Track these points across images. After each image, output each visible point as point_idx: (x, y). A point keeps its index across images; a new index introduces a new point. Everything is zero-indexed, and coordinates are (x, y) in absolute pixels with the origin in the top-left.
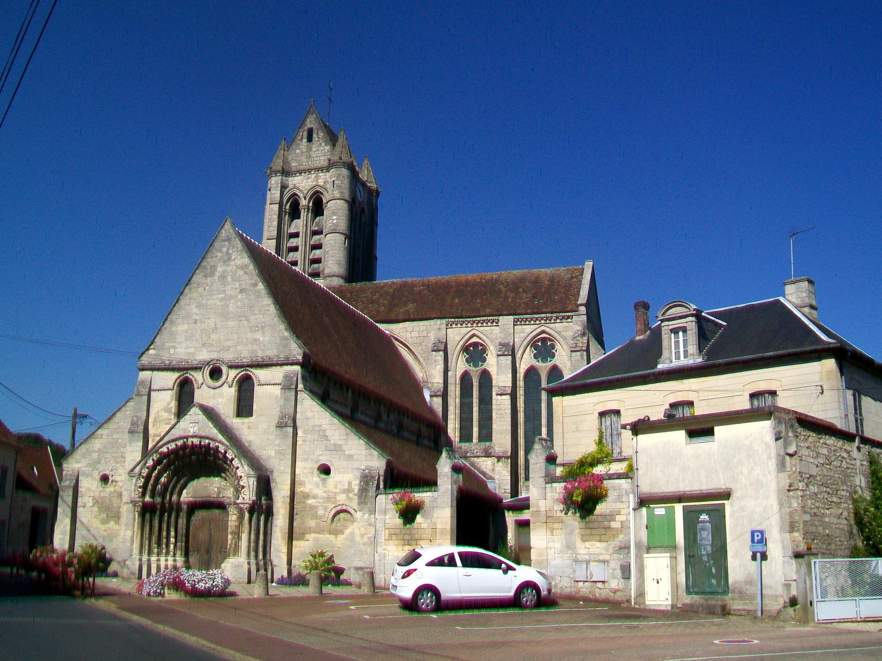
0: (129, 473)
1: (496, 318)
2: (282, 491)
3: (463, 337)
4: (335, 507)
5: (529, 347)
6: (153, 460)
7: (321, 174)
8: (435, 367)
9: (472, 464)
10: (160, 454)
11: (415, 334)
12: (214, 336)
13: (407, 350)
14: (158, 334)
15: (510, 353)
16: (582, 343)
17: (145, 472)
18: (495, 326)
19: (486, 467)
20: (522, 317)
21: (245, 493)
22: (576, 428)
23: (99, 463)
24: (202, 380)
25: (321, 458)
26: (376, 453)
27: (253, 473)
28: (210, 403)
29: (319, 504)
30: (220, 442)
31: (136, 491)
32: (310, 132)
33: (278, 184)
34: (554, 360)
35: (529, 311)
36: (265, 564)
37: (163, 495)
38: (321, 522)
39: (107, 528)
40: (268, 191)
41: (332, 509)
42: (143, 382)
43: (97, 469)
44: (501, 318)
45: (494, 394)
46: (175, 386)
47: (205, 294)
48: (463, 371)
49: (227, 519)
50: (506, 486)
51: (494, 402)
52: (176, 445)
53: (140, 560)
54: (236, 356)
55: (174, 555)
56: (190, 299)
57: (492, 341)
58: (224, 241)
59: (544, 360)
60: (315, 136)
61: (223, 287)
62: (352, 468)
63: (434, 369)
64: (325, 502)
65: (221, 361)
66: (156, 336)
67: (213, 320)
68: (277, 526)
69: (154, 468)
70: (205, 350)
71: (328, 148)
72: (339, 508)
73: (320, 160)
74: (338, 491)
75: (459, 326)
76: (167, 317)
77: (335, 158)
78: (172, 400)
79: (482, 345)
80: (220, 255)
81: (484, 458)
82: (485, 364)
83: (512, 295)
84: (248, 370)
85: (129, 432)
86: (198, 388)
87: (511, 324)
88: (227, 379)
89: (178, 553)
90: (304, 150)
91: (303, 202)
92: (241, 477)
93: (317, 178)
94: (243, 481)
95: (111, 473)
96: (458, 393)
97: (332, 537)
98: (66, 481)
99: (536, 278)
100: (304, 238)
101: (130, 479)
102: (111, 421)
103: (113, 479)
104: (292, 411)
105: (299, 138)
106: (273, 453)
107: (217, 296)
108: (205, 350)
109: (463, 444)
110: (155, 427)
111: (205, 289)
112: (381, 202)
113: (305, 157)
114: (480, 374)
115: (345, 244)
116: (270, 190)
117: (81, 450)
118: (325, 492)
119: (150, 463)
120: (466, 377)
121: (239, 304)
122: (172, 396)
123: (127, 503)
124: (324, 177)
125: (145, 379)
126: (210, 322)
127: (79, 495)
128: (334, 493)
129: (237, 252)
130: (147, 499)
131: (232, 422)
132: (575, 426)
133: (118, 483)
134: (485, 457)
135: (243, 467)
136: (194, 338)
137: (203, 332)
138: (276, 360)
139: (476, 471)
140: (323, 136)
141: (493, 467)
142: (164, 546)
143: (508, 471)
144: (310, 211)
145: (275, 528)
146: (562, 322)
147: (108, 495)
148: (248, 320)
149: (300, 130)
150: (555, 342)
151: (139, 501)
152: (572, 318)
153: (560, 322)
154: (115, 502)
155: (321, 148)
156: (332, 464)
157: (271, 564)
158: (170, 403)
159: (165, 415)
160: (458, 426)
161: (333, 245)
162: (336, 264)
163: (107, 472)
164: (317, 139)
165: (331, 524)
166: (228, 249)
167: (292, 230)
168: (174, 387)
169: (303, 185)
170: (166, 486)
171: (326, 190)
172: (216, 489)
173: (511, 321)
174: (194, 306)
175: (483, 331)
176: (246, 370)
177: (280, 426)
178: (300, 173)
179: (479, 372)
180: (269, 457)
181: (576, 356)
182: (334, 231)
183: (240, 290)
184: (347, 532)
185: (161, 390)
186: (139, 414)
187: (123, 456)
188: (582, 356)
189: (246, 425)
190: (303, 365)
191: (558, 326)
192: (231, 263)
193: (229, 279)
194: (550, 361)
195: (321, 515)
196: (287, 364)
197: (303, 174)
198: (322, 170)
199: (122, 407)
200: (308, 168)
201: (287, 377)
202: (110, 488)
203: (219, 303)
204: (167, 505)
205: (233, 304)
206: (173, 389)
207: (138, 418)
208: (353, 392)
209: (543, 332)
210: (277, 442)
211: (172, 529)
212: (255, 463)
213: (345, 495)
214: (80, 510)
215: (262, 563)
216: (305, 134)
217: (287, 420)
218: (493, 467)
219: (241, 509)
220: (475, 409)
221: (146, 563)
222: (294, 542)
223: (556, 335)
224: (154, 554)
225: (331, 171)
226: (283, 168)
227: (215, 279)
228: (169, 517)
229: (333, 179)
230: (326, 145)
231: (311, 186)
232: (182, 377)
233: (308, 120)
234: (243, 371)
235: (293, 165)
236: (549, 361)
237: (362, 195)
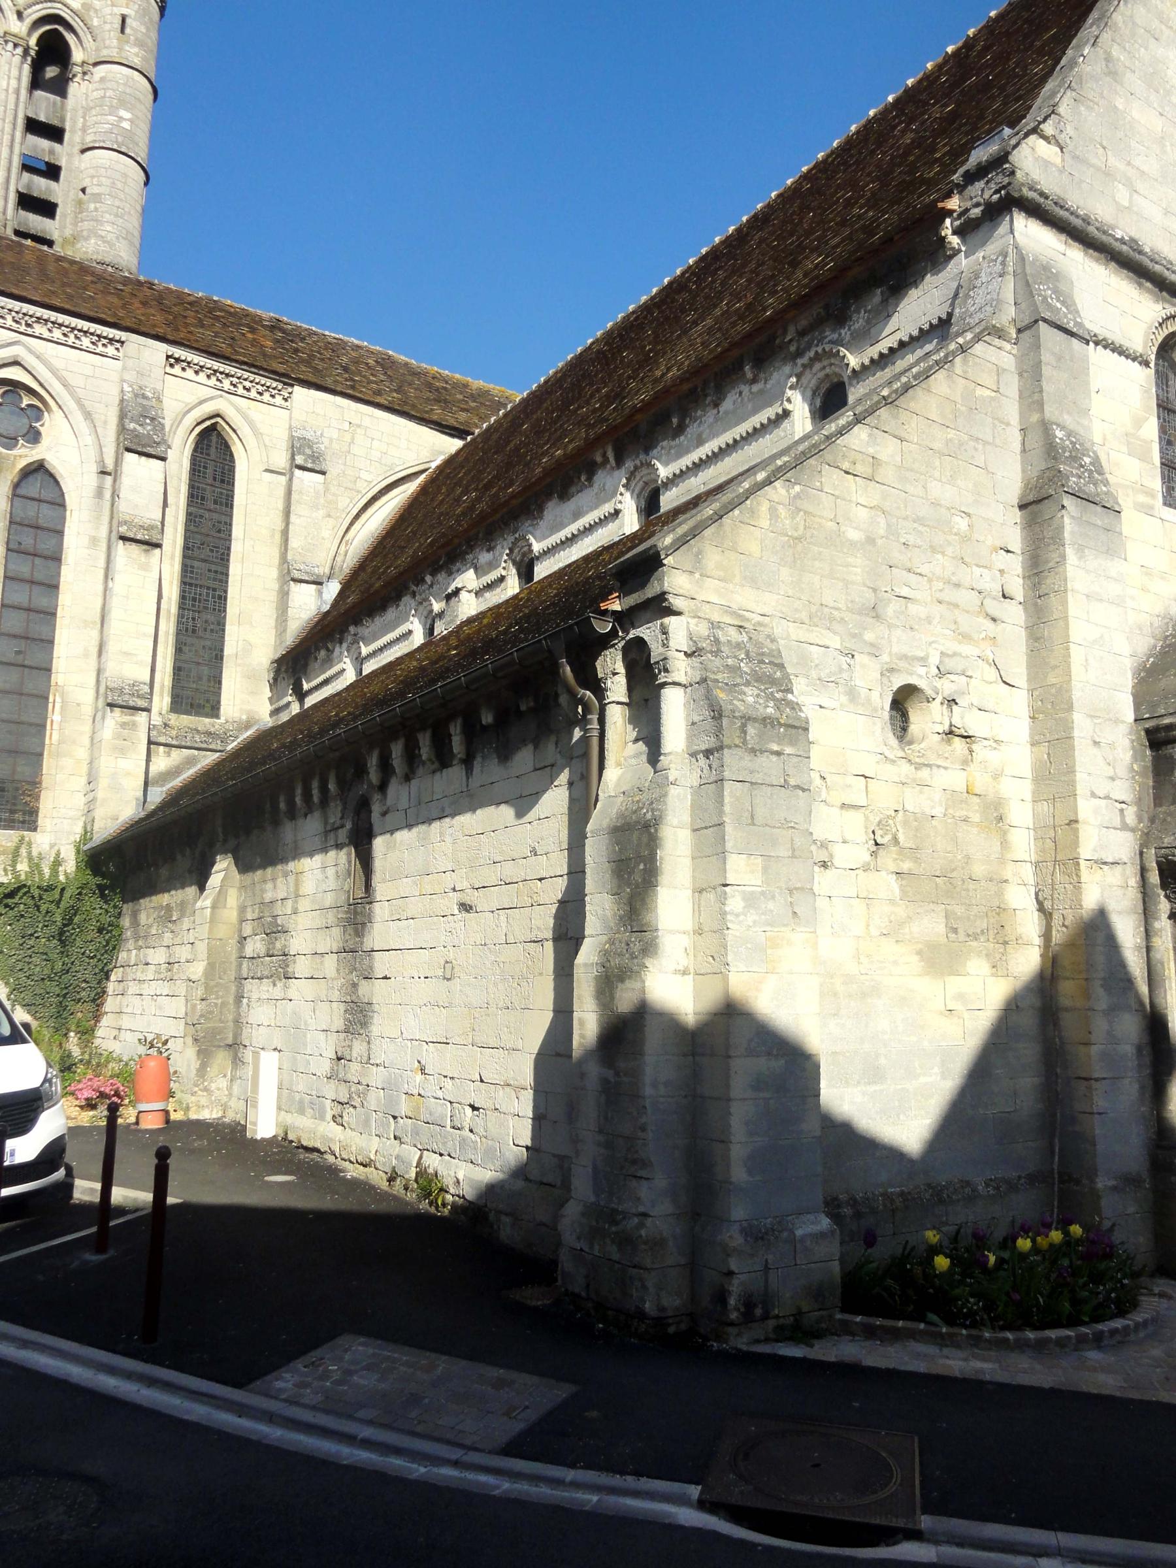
23: (874, 612)
39: (960, 997)
95: (947, 687)
144: (29, 59)
162: (125, 239)
182: (123, 149)
229: (125, 11)
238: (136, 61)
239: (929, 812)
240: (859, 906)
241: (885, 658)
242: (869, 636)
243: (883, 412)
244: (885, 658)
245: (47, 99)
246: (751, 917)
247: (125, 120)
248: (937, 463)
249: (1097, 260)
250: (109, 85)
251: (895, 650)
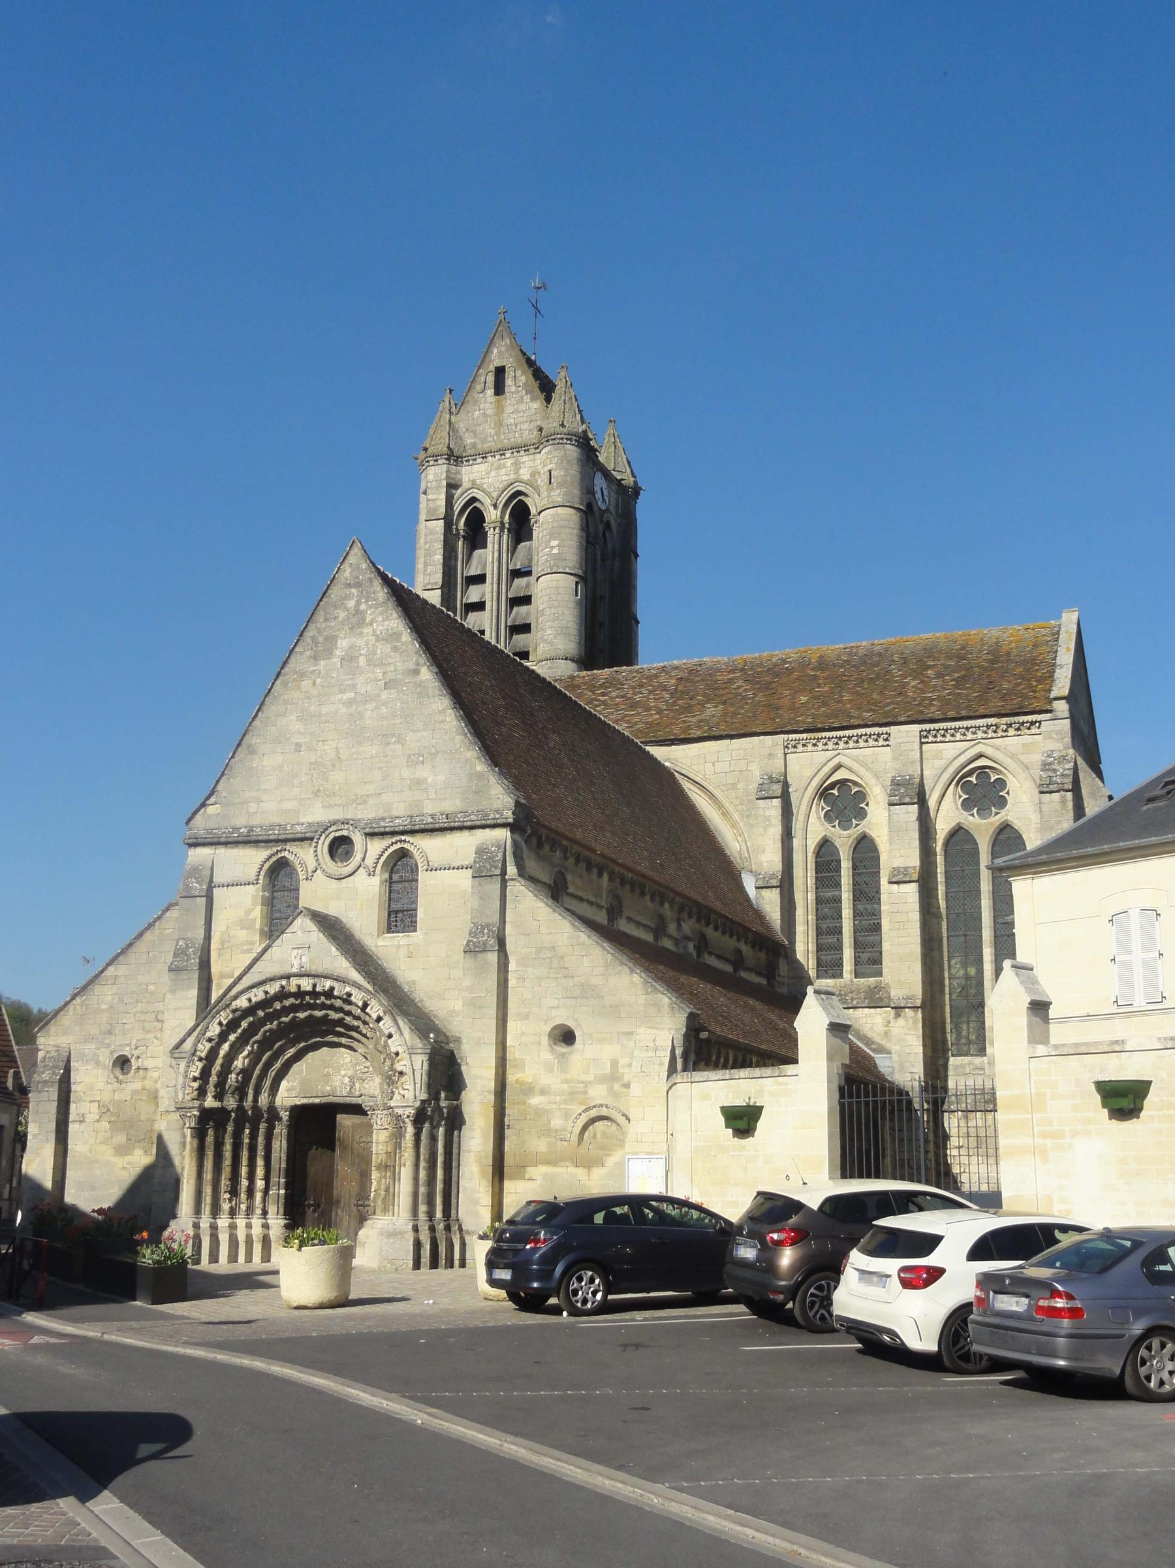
0: (172, 1052)
1: (884, 730)
2: (479, 1081)
3: (819, 771)
4: (586, 1110)
5: (952, 786)
6: (220, 1024)
7: (525, 458)
8: (765, 831)
10: (234, 1011)
12: (337, 776)
13: (707, 799)
14: (222, 775)
15: (916, 801)
16: (1062, 775)
17: (204, 1048)
18: (883, 746)
19: (871, 1029)
21: (405, 1087)
23: (110, 1033)
24: (315, 864)
25: (554, 1013)
26: (667, 1000)
27: (420, 1046)
28: (331, 909)
29: (554, 1106)
30: (355, 985)
31: (188, 1088)
32: (500, 372)
33: (440, 480)
34: (1003, 812)
35: (952, 714)
36: (448, 1228)
37: (241, 1091)
38: (559, 1142)
39: (129, 1163)
40: (422, 496)
41: (580, 1114)
42: (195, 871)
43: (108, 1045)
44: (893, 729)
45: (884, 881)
46: (261, 877)
47: (315, 692)
48: (820, 837)
49: (369, 1140)
50: (913, 1066)
51: (884, 897)
52: (266, 993)
53: (196, 1226)
54: (381, 814)
55: (265, 1213)
56: (286, 702)
57: (877, 777)
58: (349, 586)
59: (983, 812)
60: (510, 383)
61: (350, 679)
62: (618, 1033)
64: (565, 1102)
65: (352, 825)
66: (220, 779)
67: (334, 744)
68: (469, 1151)
69: (223, 1037)
70: (318, 805)
71: (536, 405)
72: (593, 1113)
73: (521, 430)
74: (591, 1078)
75: (810, 747)
76: (241, 740)
77: (551, 425)
78: (254, 904)
80: (342, 615)
83: (914, 683)
84: (405, 841)
85: (171, 970)
86: (307, 879)
87: (914, 742)
88: (363, 860)
89: (272, 1209)
90: (490, 412)
91: (492, 515)
92: (397, 1054)
93: (517, 466)
94: (401, 1063)
95: (136, 1053)
96: (811, 882)
97: (580, 1172)
98: (43, 1073)
99: (963, 648)
100: (495, 586)
101: (174, 1062)
102: (134, 950)
103: (140, 1064)
104: (496, 918)
105: (479, 387)
106: (458, 1005)
107: (340, 696)
108: (318, 805)
110: (221, 958)
111: (314, 684)
112: (643, 509)
113: (493, 425)
114: (854, 845)
115: (577, 595)
116: (425, 493)
117: (75, 1009)
118: (565, 1081)
119: (215, 1030)
120: (825, 845)
121: (384, 709)
122: (254, 897)
123: (167, 1111)
124: (531, 464)
125: (200, 865)
126: (325, 748)
127: (73, 1097)
128: (583, 1082)
129: (377, 608)
130: (210, 1102)
131: (377, 946)
133: (150, 1074)
135: (401, 1034)
136: (296, 782)
137: (314, 769)
138: (462, 819)
140: (524, 384)
141: (886, 1029)
142: (243, 1196)
143: (918, 1037)
145: (466, 1155)
146: (1020, 735)
147: (128, 1098)
148: (400, 740)
149: (481, 371)
150: (1005, 775)
151: (194, 1108)
152: (1040, 724)
153: (1014, 736)
154: (145, 1110)
155: (523, 407)
156: (578, 1024)
157: (461, 1230)
158: (252, 910)
159: (242, 934)
160: (812, 947)
161: (554, 597)
163: (126, 1052)
164: (513, 389)
165: (579, 1143)
166: (358, 603)
167: (474, 571)
168: (258, 879)
169: (490, 480)
170: (246, 1073)
171: (536, 489)
172: (347, 1080)
173: (915, 736)
174: (293, 718)
176: (401, 841)
177: (472, 950)
178: (483, 458)
179: (851, 840)
180: (452, 1013)
181: (1051, 802)
182: (553, 571)
183: (385, 683)
184: (611, 1161)
185: (233, 885)
186: (189, 935)
187: (160, 1019)
188: (1063, 801)
189: (403, 952)
190: (513, 827)
191: (1012, 742)
192: (365, 630)
193: (362, 661)
194: (997, 814)
195: (558, 1127)
196: (483, 827)
197: (490, 458)
198: (525, 451)
199: (155, 921)
200: (499, 446)
201: (480, 851)
202: (133, 1084)
203: (343, 710)
204: (250, 1112)
205: (372, 710)
206: (257, 883)
207: (189, 942)
208: (611, 880)
209: (980, 756)
210: (467, 982)
211: (260, 1162)
212: (423, 1023)
213: (605, 1086)
214: (73, 1128)
215: (441, 1226)
216: (491, 378)
217: (485, 938)
218: (886, 1029)
219: (398, 1117)
220: (847, 912)
221: (208, 1232)
222: (507, 1184)
223: (1007, 761)
224: (223, 1214)
225: (543, 451)
226: (449, 447)
227: (334, 663)
228: (254, 1136)
229: (549, 468)
231: (505, 483)
232: (274, 859)
233: (495, 351)
234: (396, 843)
235: (468, 442)
236: (993, 813)
237: (607, 499)
238: (559, 499)
239: (124, 1099)
240: (94, 1134)
241: (113, 1047)
242: (107, 1041)
243: (121, 958)
244: (113, 1047)
245: (525, 546)
246: (34, 1141)
247: (554, 547)
248: (143, 968)
249: (232, 848)
250: (544, 527)
251: (117, 1043)
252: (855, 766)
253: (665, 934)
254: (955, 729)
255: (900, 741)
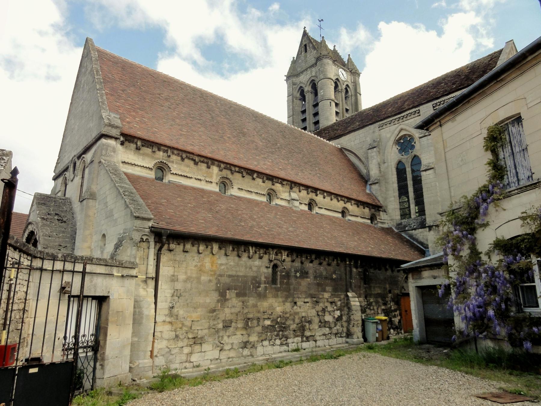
1: (417, 109)
9: (411, 236)
11: (357, 141)
20: (439, 100)
22: (462, 160)
44: (421, 108)
63: (371, 164)
79: (410, 136)
81: (420, 230)
82: (415, 150)
93: (311, 72)
109: (403, 221)
132: (460, 159)
134: (421, 228)
139: (414, 242)
155: (312, 53)
175: (408, 123)
230: (314, 50)
252: (407, 128)
253: (278, 198)
254: (448, 99)
255: (424, 111)
